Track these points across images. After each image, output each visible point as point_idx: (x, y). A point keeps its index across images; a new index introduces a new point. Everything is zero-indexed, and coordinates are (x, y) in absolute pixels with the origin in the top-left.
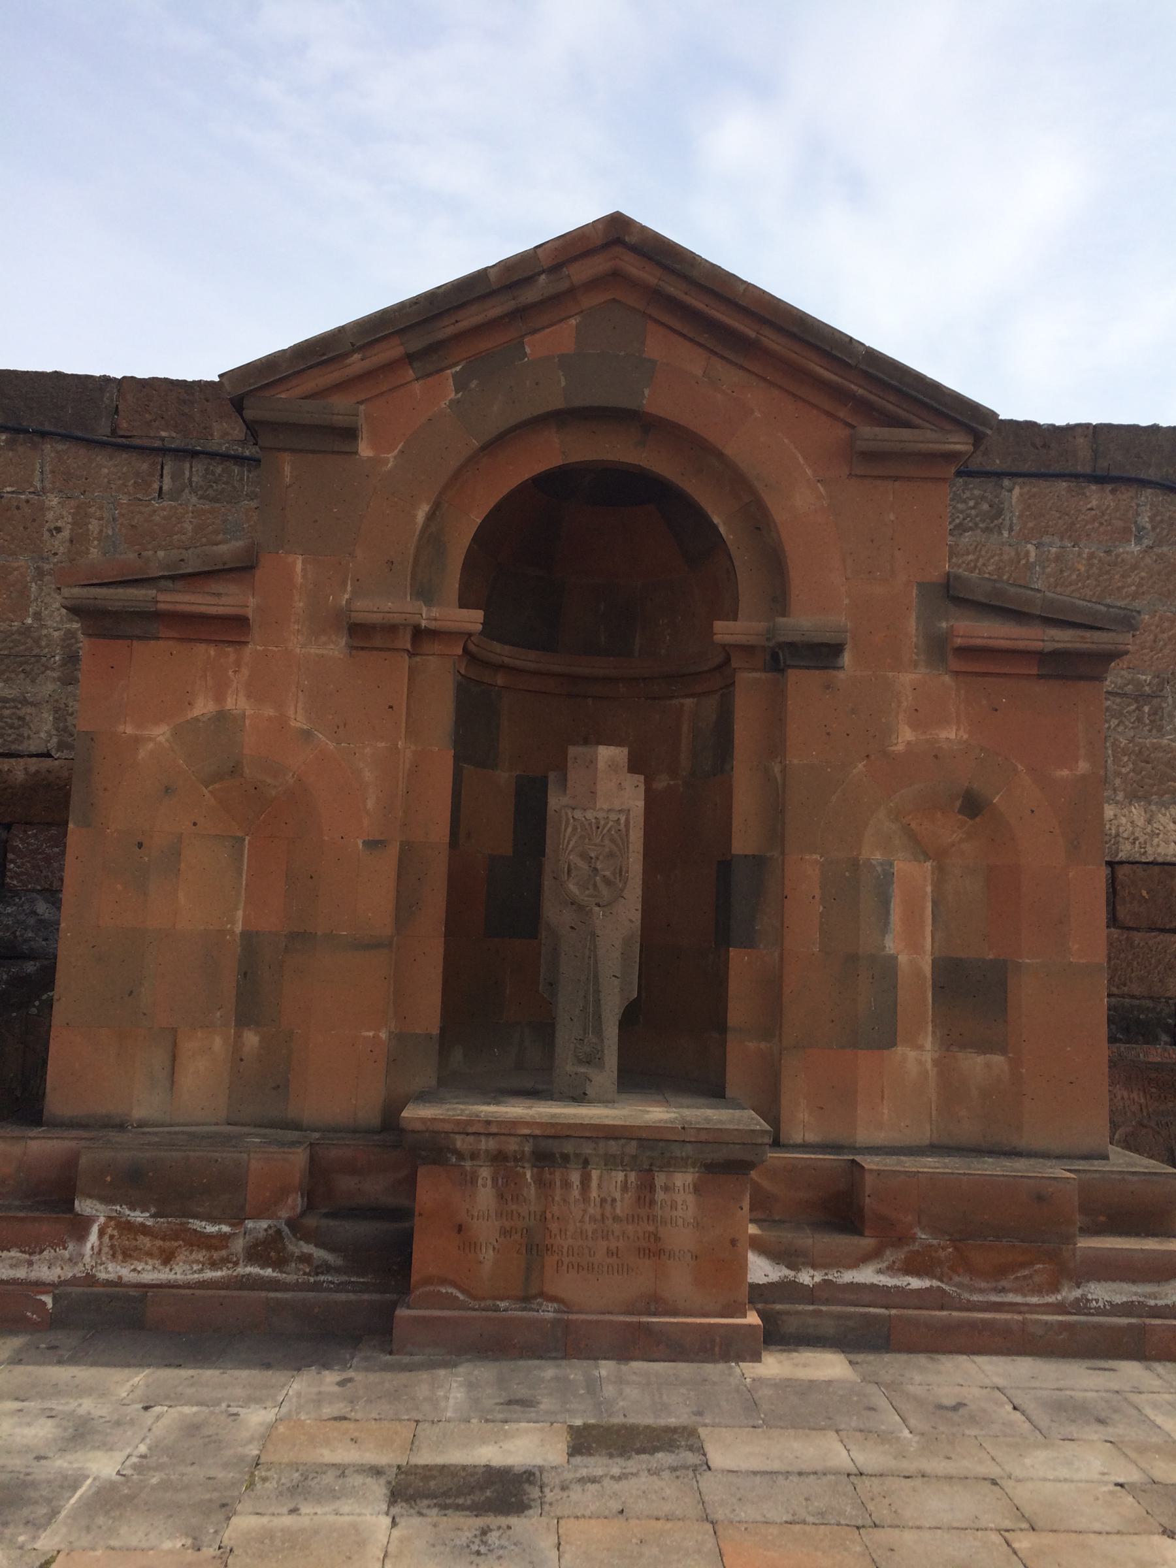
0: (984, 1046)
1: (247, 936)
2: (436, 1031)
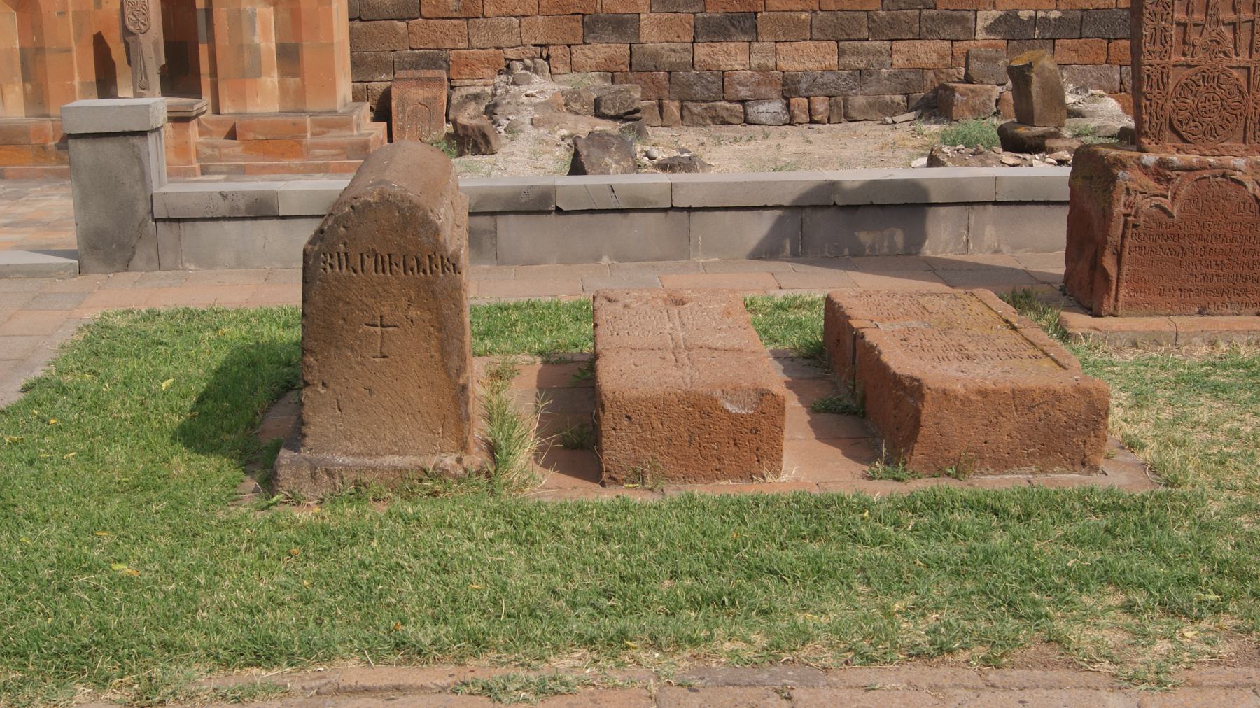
0: (294, 76)
1: (21, 49)
2: (94, 80)
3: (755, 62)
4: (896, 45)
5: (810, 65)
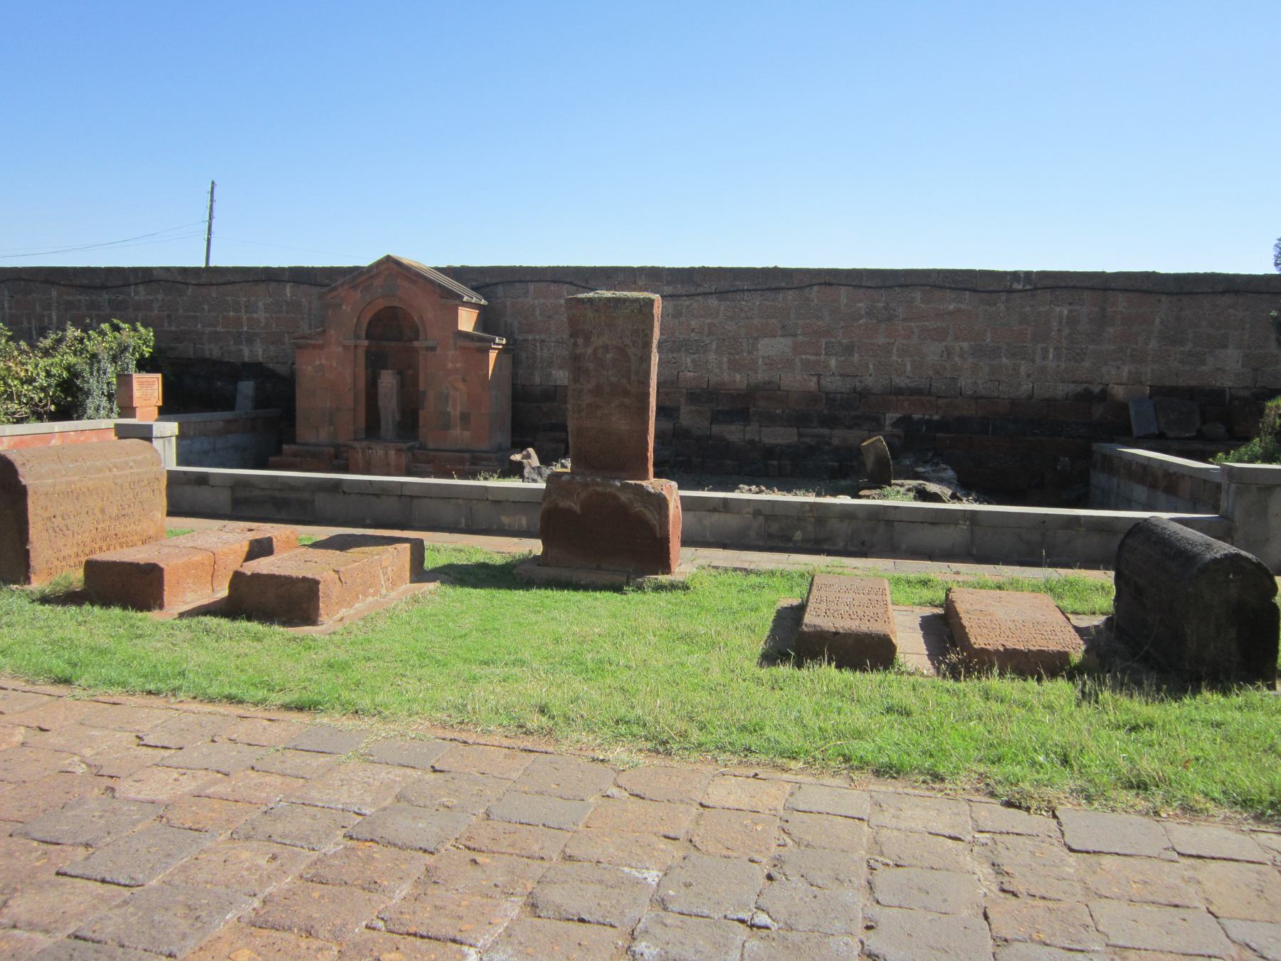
3: (748, 437)
4: (836, 432)
5: (780, 441)
